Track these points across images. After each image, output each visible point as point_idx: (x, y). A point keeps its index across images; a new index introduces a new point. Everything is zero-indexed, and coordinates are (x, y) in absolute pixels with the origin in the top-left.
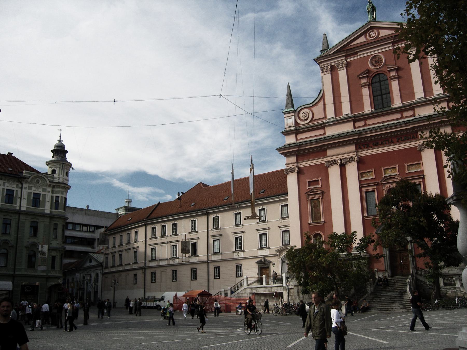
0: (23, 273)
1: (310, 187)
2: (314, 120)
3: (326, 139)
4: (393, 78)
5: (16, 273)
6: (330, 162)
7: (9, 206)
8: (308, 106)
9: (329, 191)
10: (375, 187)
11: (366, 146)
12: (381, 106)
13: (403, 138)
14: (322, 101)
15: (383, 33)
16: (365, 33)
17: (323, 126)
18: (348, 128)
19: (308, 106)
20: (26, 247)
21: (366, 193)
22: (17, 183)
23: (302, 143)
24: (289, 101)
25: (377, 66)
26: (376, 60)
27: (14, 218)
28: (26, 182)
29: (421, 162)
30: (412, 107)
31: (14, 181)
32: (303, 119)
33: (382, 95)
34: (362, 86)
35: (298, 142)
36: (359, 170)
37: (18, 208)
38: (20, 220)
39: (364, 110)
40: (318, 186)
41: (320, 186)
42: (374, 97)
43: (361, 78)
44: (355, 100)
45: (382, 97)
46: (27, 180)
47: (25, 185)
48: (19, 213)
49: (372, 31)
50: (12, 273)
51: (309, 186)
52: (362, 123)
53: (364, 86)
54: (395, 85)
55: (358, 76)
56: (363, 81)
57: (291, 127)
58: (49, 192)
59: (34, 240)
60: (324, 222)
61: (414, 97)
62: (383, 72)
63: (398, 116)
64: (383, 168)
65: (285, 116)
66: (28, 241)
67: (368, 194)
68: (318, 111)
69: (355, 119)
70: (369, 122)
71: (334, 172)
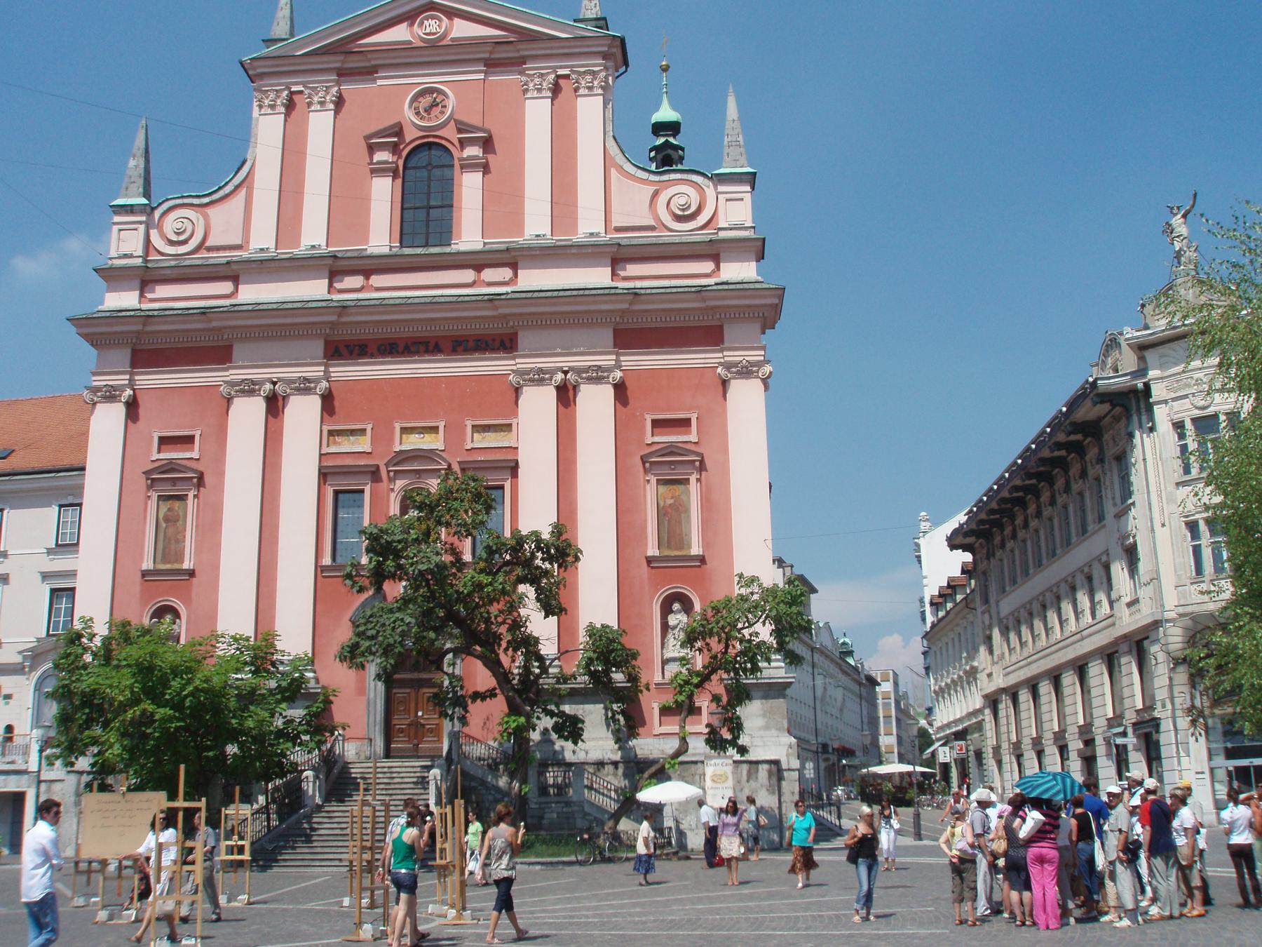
1: (162, 456)
2: (210, 249)
4: (468, 166)
6: (238, 384)
8: (196, 201)
9: (221, 474)
10: (367, 479)
11: (356, 351)
13: (471, 344)
15: (463, 29)
16: (410, 17)
17: (233, 273)
19: (196, 201)
21: (337, 493)
23: (156, 313)
24: (136, 173)
25: (430, 120)
29: (514, 422)
30: (512, 259)
32: (174, 238)
34: (373, 171)
35: (145, 306)
39: (366, 241)
40: (188, 455)
41: (195, 455)
42: (403, 209)
44: (346, 207)
45: (428, 214)
49: (433, 18)
51: (159, 452)
52: (355, 281)
53: (377, 171)
54: (470, 187)
55: (367, 138)
56: (382, 156)
57: (131, 256)
60: (192, 573)
61: (519, 227)
62: (443, 142)
63: (468, 275)
64: (397, 426)
65: (117, 219)
67: (341, 496)
68: (223, 224)
70: (376, 280)
71: (247, 416)
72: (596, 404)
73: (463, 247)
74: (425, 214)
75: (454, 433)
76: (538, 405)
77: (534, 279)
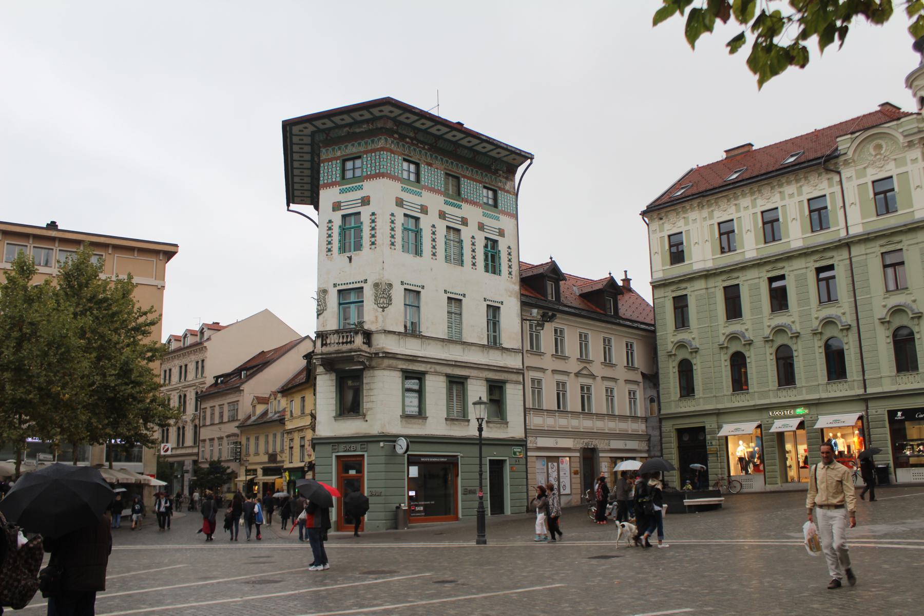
0: (888, 386)
5: (869, 391)
7: (822, 238)
20: (883, 322)
22: (829, 176)
27: (839, 260)
28: (846, 163)
31: (819, 175)
37: (843, 234)
38: (853, 260)
46: (842, 158)
47: (846, 172)
48: (846, 244)
50: (861, 391)
58: (915, 161)
59: (897, 300)
66: (885, 306)
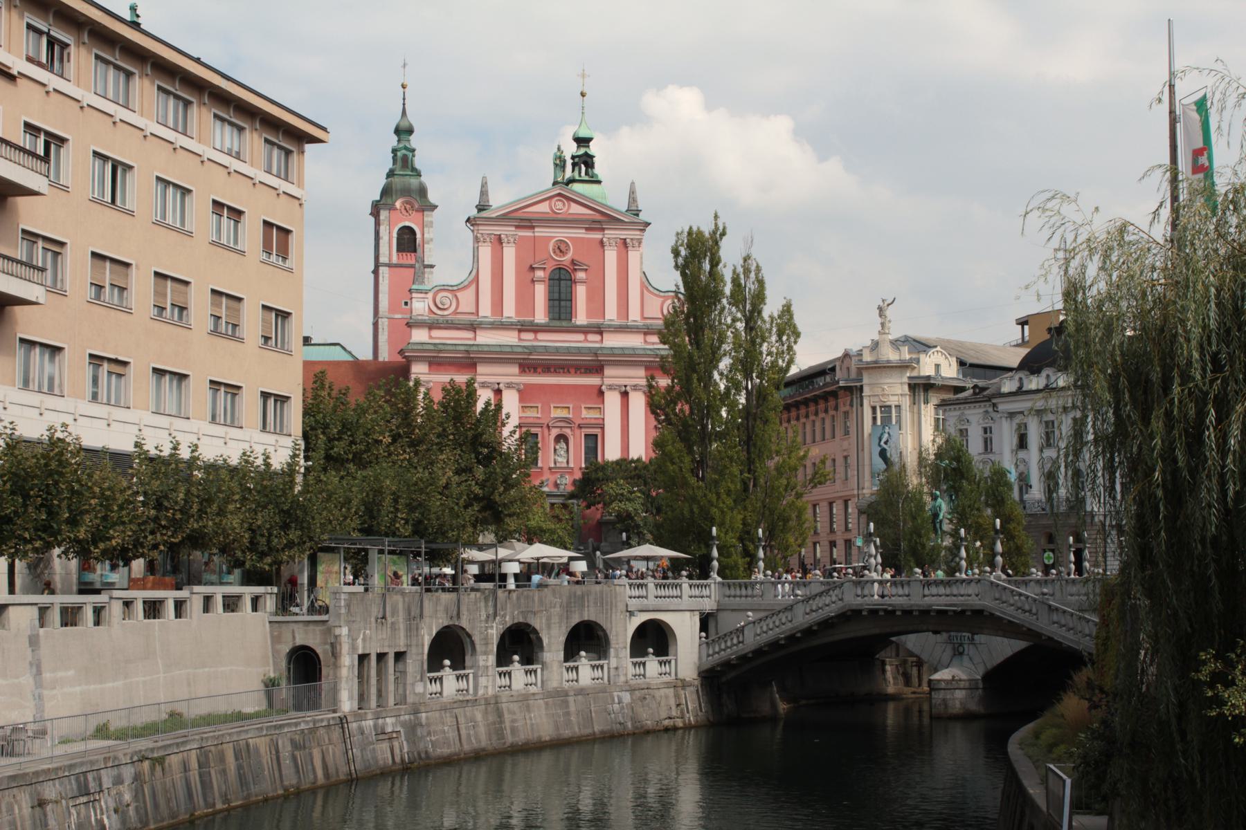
3: (481, 349)
4: (582, 282)
12: (557, 316)
14: (473, 287)
15: (576, 209)
17: (473, 327)
18: (509, 338)
26: (561, 248)
30: (599, 330)
33: (560, 300)
36: (521, 400)
43: (532, 269)
44: (525, 300)
52: (530, 336)
54: (581, 292)
63: (581, 337)
68: (466, 301)
69: (524, 327)
70: (541, 336)
72: (638, 402)
73: (578, 323)
74: (561, 305)
75: (577, 410)
76: (612, 401)
77: (613, 341)
